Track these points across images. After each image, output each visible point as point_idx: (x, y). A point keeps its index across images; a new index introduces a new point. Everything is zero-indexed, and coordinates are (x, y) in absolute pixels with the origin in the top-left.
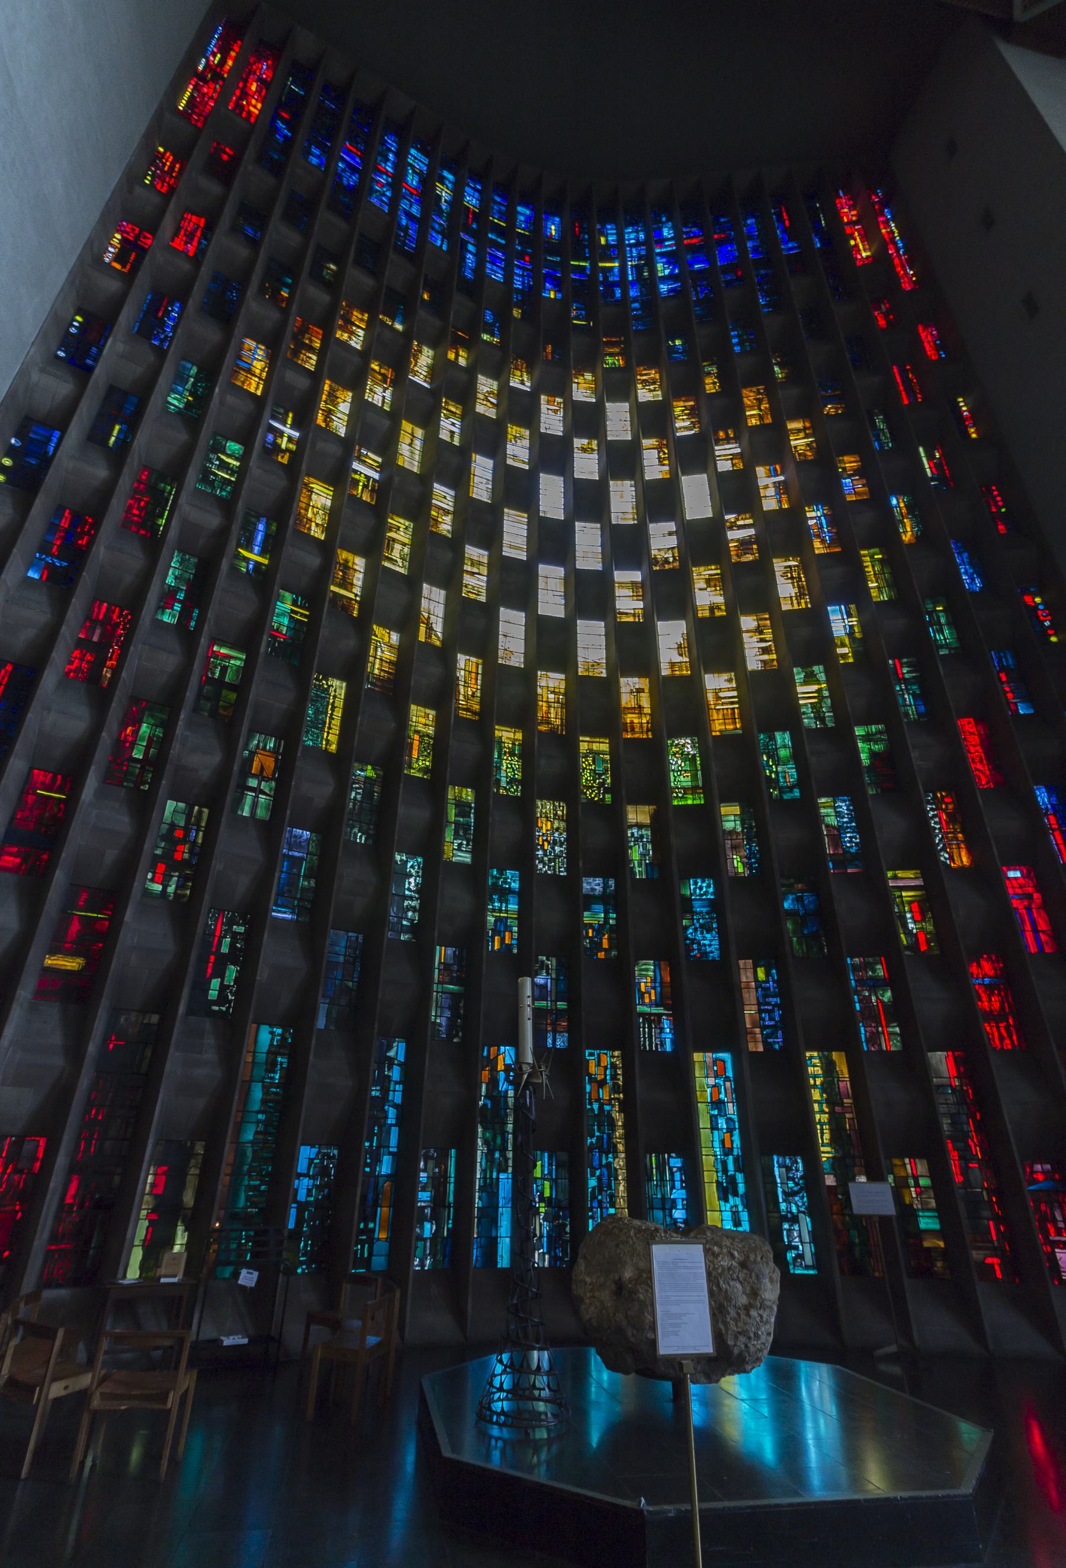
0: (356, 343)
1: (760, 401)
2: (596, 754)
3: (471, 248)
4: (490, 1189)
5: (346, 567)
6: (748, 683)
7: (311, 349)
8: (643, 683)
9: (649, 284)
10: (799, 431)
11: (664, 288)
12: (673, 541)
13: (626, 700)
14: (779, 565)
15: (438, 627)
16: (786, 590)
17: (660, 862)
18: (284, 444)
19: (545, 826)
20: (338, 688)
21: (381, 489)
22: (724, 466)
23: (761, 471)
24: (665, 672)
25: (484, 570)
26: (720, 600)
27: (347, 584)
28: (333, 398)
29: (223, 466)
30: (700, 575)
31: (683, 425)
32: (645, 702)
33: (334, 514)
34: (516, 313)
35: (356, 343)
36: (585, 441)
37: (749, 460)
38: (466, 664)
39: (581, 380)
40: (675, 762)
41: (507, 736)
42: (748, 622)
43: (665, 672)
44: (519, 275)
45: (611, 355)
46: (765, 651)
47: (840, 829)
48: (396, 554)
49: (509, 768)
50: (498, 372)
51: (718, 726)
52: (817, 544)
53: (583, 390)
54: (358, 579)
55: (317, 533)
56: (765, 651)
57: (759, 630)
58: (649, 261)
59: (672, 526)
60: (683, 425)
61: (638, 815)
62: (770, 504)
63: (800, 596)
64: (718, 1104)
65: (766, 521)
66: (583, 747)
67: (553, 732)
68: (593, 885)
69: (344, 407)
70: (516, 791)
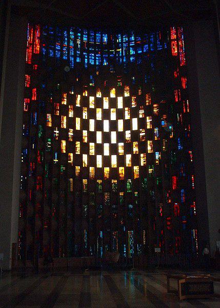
0: (65, 103)
1: (149, 98)
2: (115, 183)
3: (86, 57)
4: (99, 249)
5: (70, 156)
6: (141, 168)
7: (58, 110)
8: (123, 168)
9: (128, 56)
10: (156, 107)
11: (131, 59)
12: (130, 136)
13: (120, 172)
14: (149, 142)
15: (86, 163)
16: (149, 148)
17: (124, 202)
18: (57, 135)
19: (106, 197)
20: (71, 179)
21: (73, 137)
22: (141, 116)
23: (147, 118)
24: (127, 166)
25: (94, 148)
26: (137, 150)
27: (70, 160)
28: (63, 119)
29: (49, 145)
30: (135, 143)
31: (134, 105)
32: (123, 172)
33: (66, 147)
34: (97, 73)
35: (65, 103)
36: (113, 109)
37: (146, 114)
38: (91, 169)
39: (112, 91)
40: (128, 184)
41: (99, 181)
42: (142, 155)
43: (127, 166)
44: (98, 60)
45: (119, 82)
46: (144, 162)
47: (153, 196)
48: (78, 151)
49: (100, 187)
50: (94, 95)
51: (135, 177)
52: (156, 137)
53: (113, 94)
54: (72, 158)
55: (64, 152)
56: (144, 162)
57: (144, 157)
58: (128, 50)
59: (129, 132)
60: (134, 105)
61: (121, 194)
62: (148, 127)
63: (152, 150)
64: (131, 238)
65: (147, 131)
66: (112, 182)
67: (108, 179)
68: (114, 206)
69: (65, 120)
70: (101, 192)
